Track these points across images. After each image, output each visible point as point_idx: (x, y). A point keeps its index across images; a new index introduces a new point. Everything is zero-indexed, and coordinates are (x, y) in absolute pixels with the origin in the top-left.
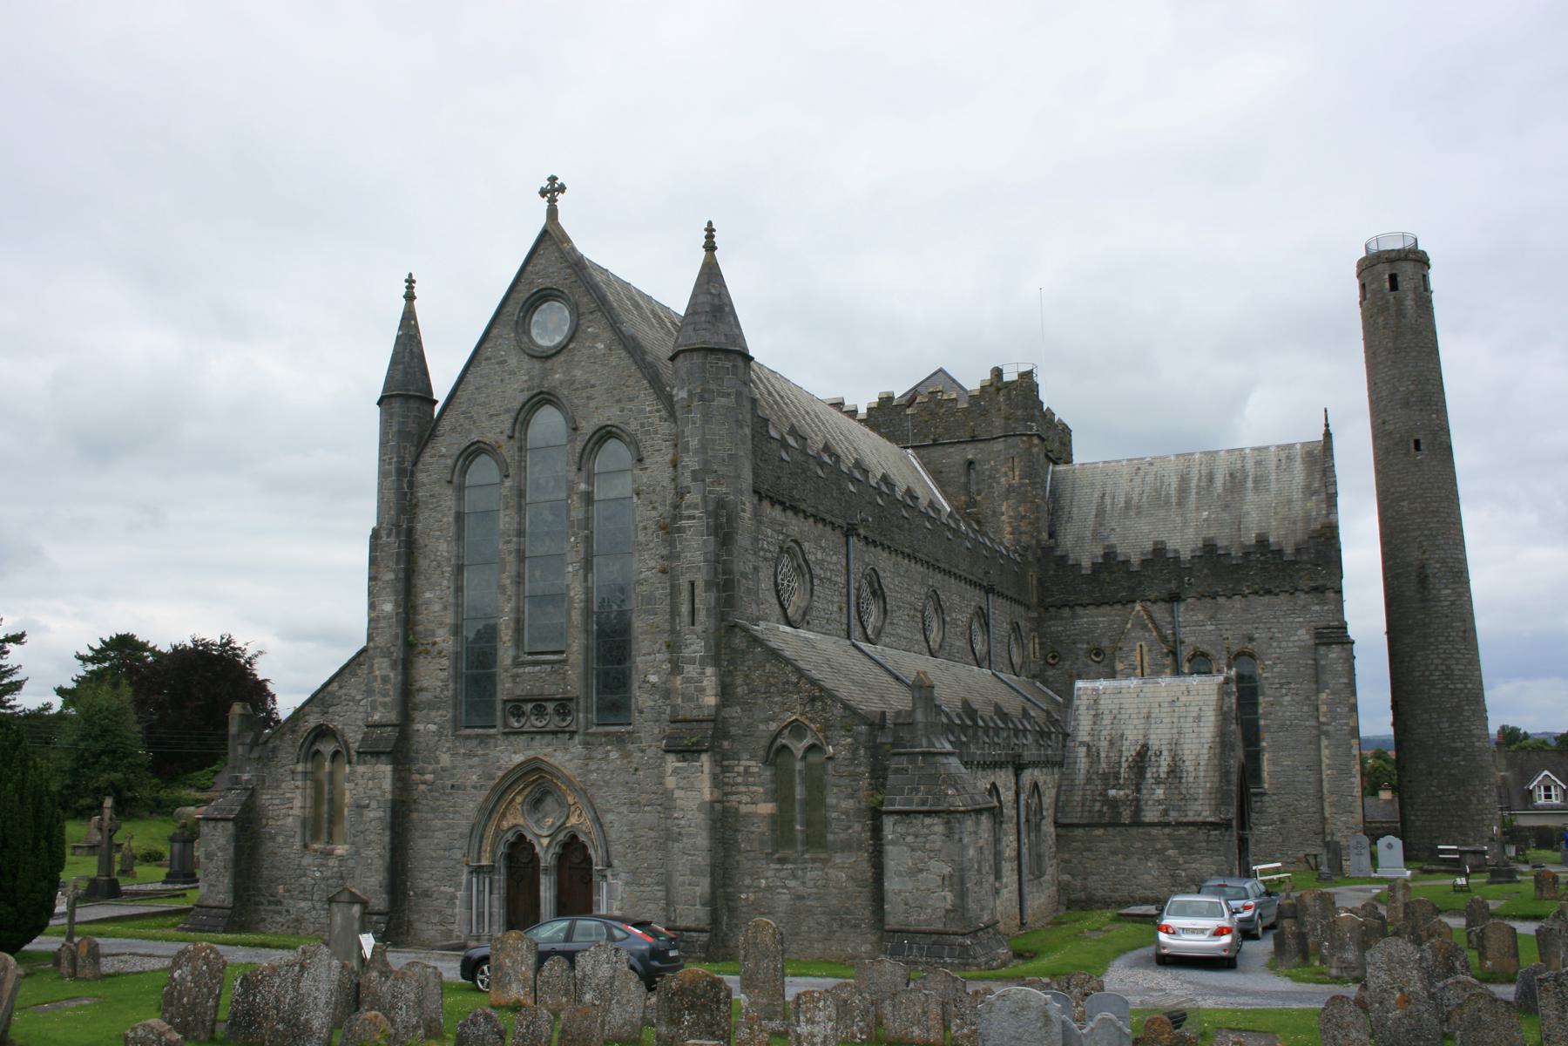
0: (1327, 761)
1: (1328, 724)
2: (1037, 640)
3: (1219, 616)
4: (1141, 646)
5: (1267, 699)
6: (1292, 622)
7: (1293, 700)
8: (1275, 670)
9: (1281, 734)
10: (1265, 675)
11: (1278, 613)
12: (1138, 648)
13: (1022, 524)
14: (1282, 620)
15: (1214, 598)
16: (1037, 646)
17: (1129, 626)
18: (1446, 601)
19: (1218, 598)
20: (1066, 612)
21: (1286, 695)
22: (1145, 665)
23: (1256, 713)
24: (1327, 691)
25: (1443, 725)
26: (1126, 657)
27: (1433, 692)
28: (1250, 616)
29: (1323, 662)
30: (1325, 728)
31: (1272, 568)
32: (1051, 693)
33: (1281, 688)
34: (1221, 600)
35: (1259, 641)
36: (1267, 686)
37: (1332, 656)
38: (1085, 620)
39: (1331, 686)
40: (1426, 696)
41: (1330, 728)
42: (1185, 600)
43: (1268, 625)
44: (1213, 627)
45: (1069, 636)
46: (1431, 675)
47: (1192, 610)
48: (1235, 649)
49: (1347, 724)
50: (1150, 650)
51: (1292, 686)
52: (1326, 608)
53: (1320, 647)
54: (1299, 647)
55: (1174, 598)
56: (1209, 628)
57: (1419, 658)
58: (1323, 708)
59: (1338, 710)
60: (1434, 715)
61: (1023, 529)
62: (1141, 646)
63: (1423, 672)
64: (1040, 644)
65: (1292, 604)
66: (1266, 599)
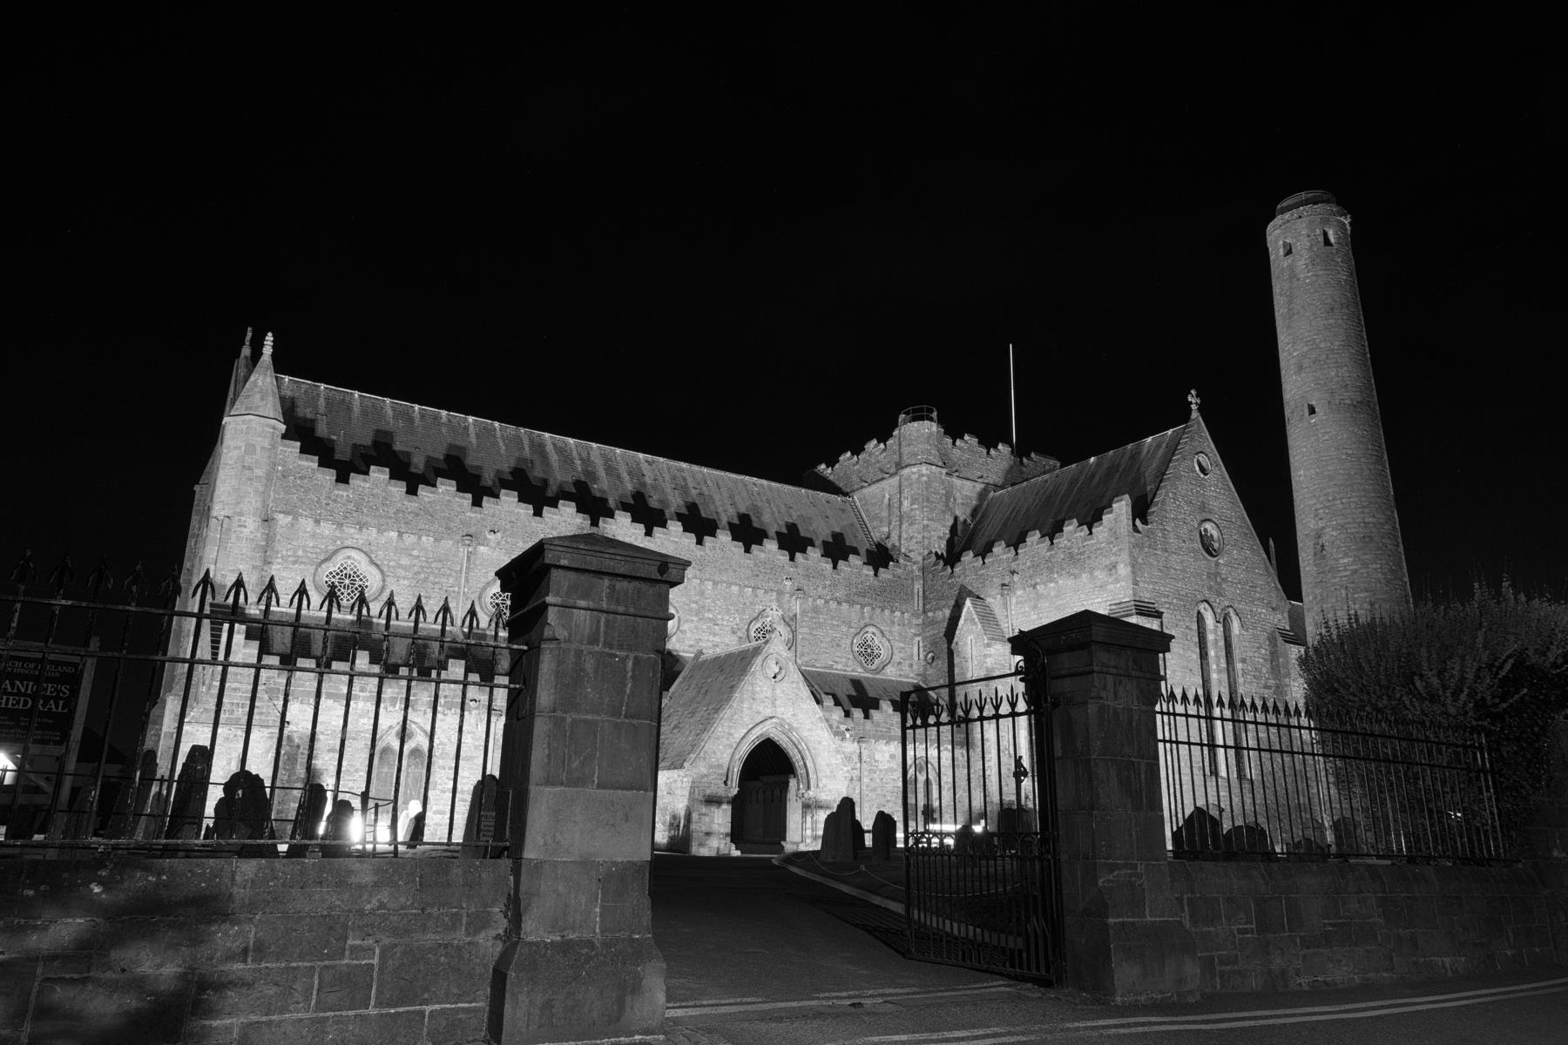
18: (1345, 570)
31: (1076, 551)
44: (1036, 616)
47: (1021, 602)
52: (1118, 585)
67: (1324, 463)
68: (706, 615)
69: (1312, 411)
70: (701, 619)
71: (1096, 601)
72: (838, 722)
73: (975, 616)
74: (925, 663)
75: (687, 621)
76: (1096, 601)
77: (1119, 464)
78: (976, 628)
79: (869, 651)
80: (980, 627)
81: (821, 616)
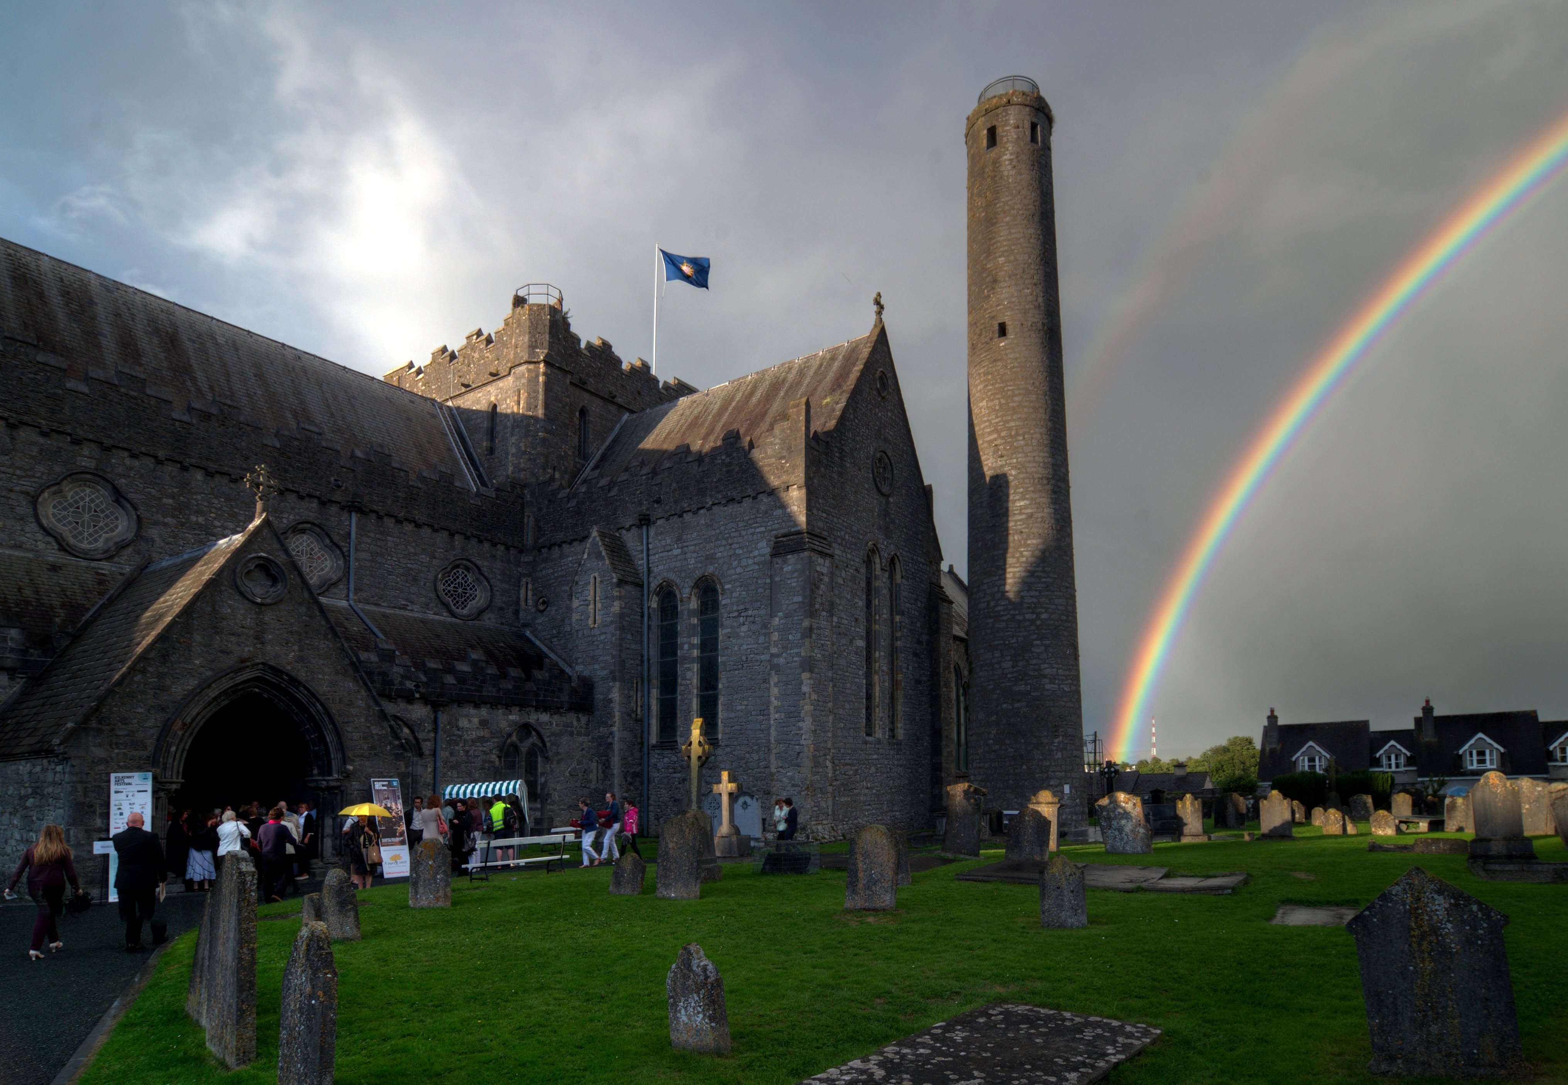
0: (775, 702)
1: (778, 656)
2: (530, 586)
3: (685, 536)
4: (595, 578)
5: (725, 631)
6: (753, 534)
7: (750, 630)
8: (734, 595)
9: (737, 672)
10: (724, 602)
11: (741, 524)
12: (592, 581)
13: (521, 460)
14: (744, 533)
15: (681, 516)
16: (530, 593)
17: (585, 556)
19: (685, 515)
20: (556, 551)
21: (744, 624)
22: (597, 598)
23: (716, 649)
24: (780, 614)
25: (1004, 665)
26: (581, 592)
27: (997, 625)
28: (713, 533)
29: (777, 579)
30: (775, 661)
32: (538, 643)
33: (739, 616)
34: (687, 517)
35: (720, 561)
36: (726, 615)
37: (787, 568)
38: (570, 559)
39: (784, 607)
40: (989, 631)
41: (781, 661)
42: (654, 523)
43: (730, 541)
44: (679, 550)
45: (556, 578)
46: (997, 605)
47: (662, 533)
48: (698, 574)
49: (798, 654)
50: (601, 582)
51: (750, 613)
53: (775, 560)
54: (758, 564)
55: (645, 521)
56: (677, 552)
57: (985, 587)
58: (775, 636)
59: (790, 637)
60: (997, 654)
61: (522, 466)
62: (595, 578)
63: (988, 602)
64: (534, 590)
65: (754, 511)
66: (729, 509)
67: (1010, 393)
68: (193, 518)
69: (1003, 330)
70: (183, 524)
71: (758, 530)
72: (402, 676)
73: (602, 548)
74: (533, 610)
75: (156, 523)
76: (758, 530)
77: (784, 380)
78: (603, 564)
79: (460, 590)
80: (607, 562)
81: (389, 538)
